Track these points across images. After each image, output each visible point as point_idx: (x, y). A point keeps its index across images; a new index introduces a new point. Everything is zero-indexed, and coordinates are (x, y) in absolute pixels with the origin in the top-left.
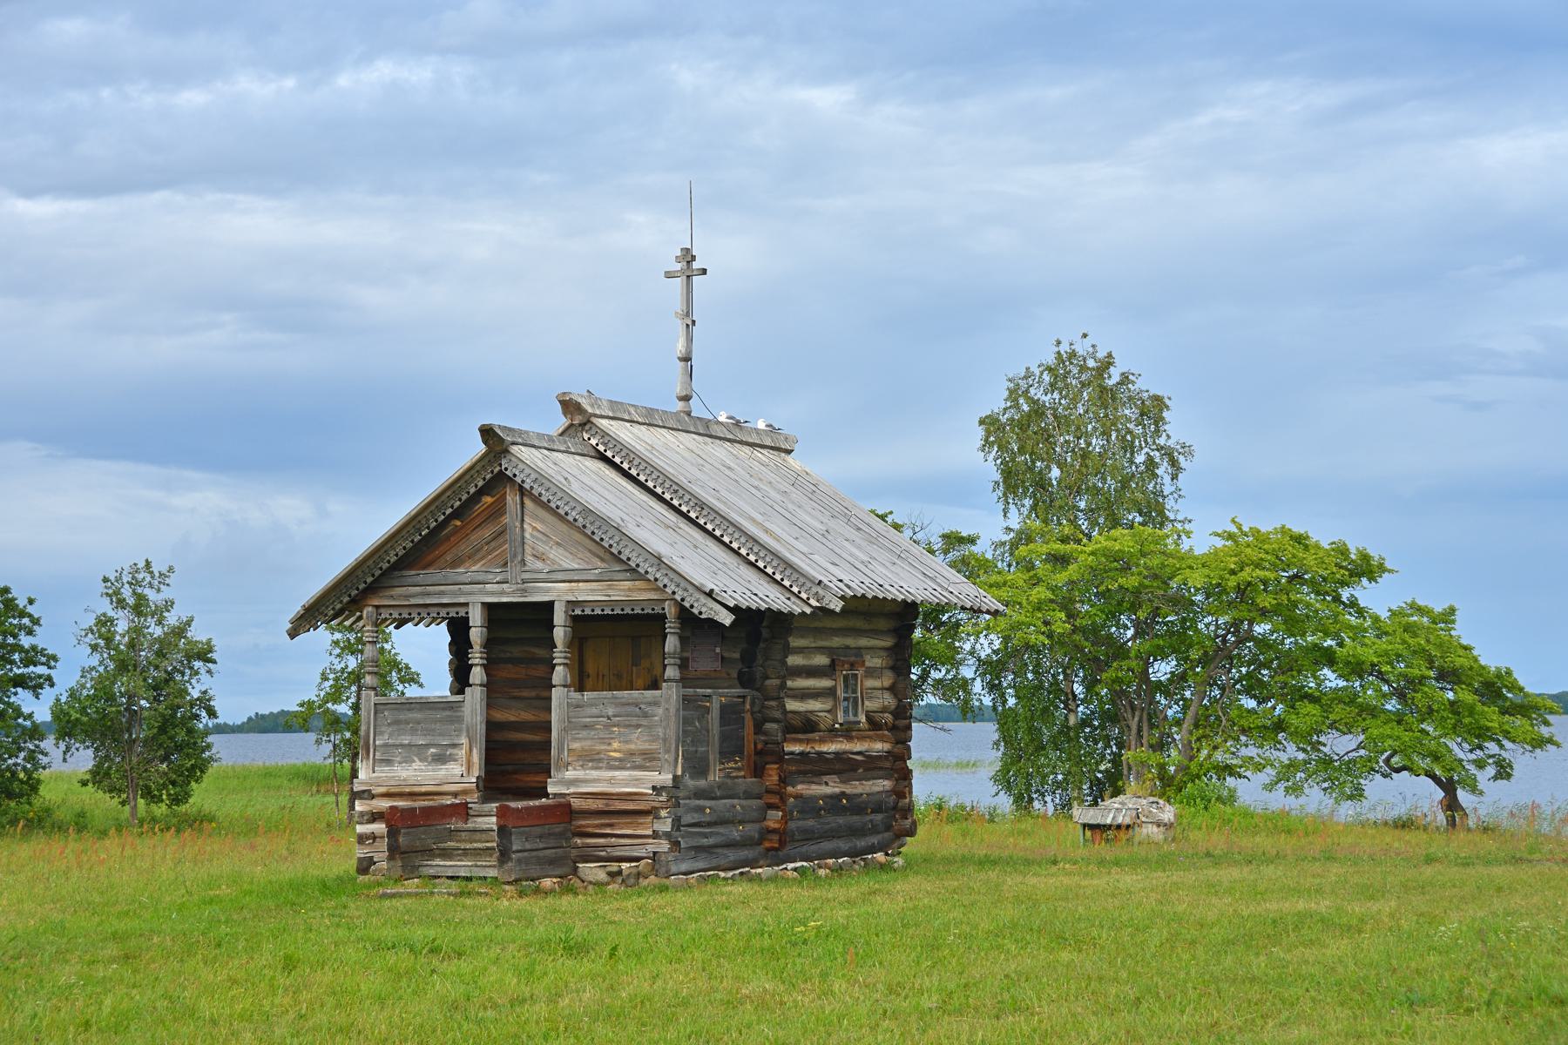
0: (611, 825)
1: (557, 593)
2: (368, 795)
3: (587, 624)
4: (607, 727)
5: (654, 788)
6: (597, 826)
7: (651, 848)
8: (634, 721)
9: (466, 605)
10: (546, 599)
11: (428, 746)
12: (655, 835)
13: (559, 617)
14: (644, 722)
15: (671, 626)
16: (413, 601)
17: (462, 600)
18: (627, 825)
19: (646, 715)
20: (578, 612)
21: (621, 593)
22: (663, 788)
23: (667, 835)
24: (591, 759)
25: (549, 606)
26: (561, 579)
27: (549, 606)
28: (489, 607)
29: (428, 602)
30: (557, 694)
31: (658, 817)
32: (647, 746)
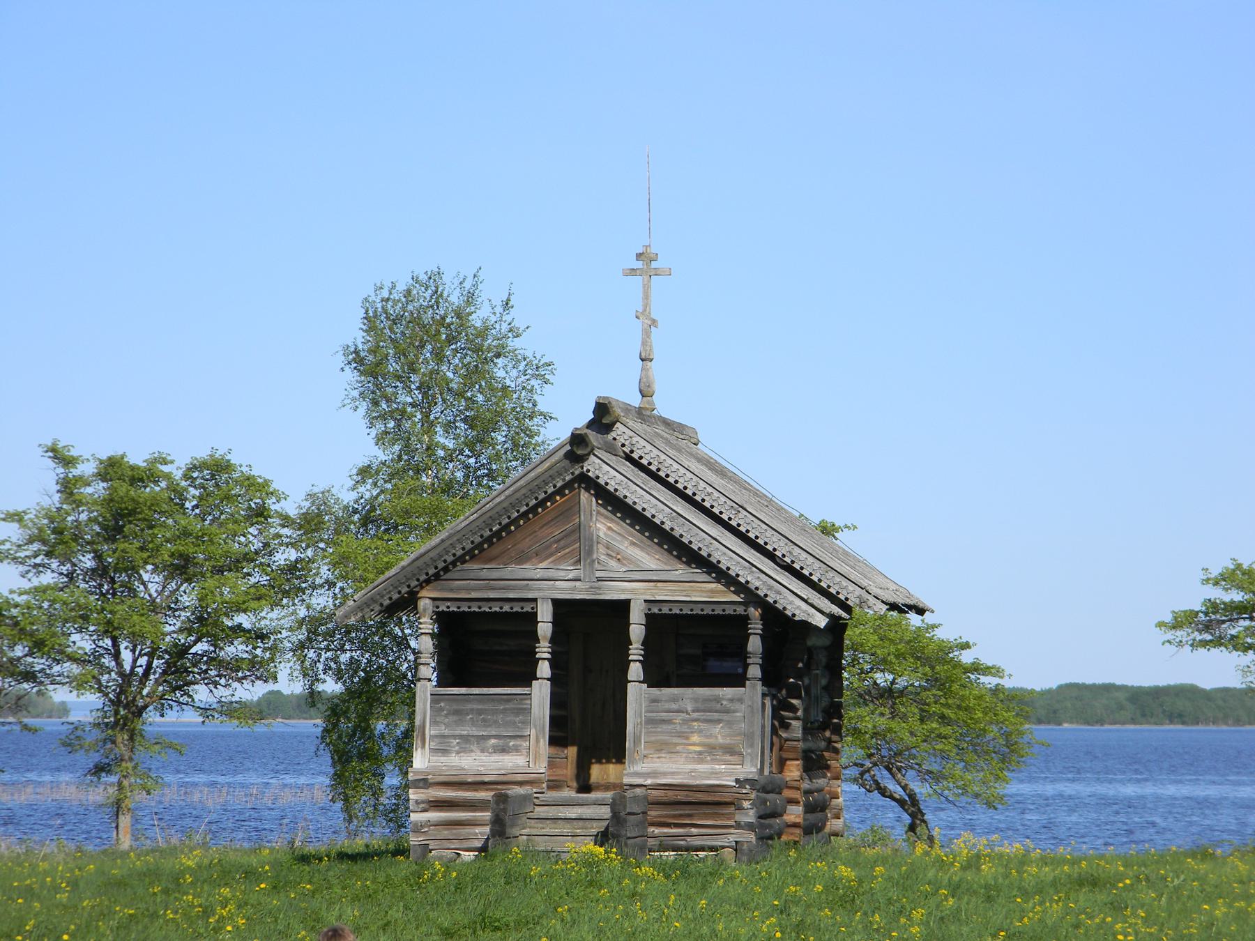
0: (690, 816)
1: (638, 595)
2: (424, 783)
3: (665, 625)
4: (685, 722)
5: (737, 781)
6: (674, 816)
7: (732, 838)
8: (716, 716)
9: (535, 600)
10: (623, 597)
11: (489, 737)
12: (738, 826)
13: (637, 618)
14: (725, 717)
15: (756, 627)
16: (474, 595)
17: (530, 596)
18: (707, 816)
19: (727, 711)
20: (443, 608)
21: (699, 591)
22: (747, 780)
23: (750, 826)
24: (662, 748)
25: (624, 606)
26: (635, 577)
27: (624, 606)
28: (557, 603)
29: (511, 596)
30: (631, 688)
31: (740, 808)
32: (728, 741)
